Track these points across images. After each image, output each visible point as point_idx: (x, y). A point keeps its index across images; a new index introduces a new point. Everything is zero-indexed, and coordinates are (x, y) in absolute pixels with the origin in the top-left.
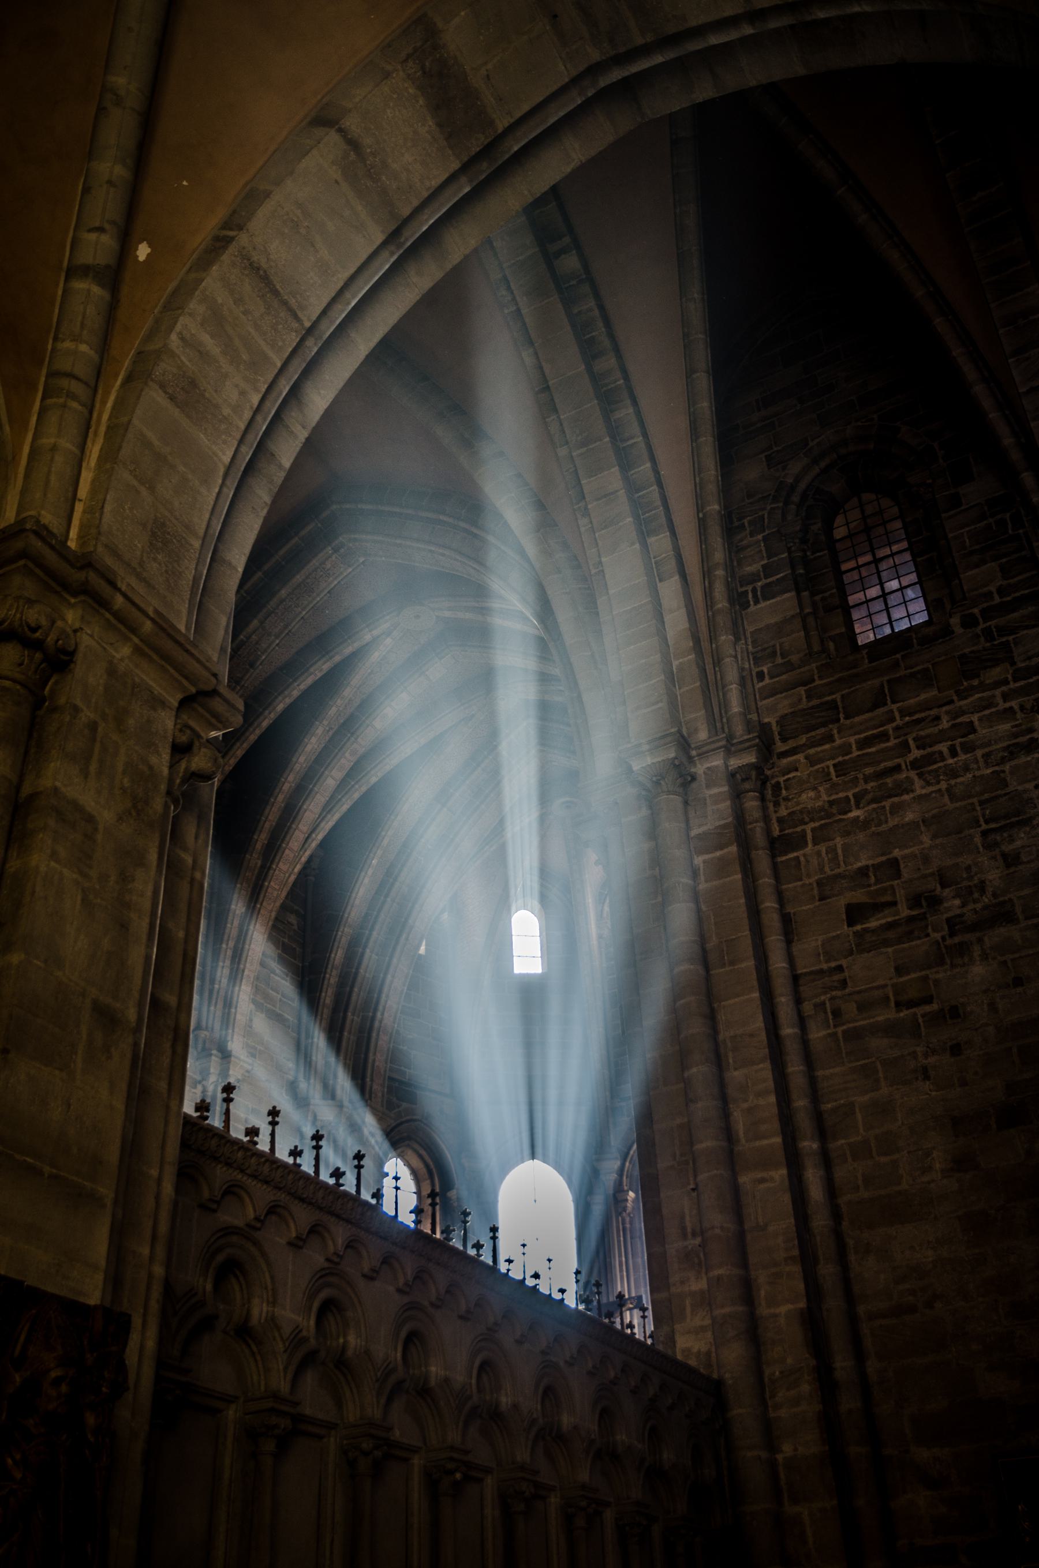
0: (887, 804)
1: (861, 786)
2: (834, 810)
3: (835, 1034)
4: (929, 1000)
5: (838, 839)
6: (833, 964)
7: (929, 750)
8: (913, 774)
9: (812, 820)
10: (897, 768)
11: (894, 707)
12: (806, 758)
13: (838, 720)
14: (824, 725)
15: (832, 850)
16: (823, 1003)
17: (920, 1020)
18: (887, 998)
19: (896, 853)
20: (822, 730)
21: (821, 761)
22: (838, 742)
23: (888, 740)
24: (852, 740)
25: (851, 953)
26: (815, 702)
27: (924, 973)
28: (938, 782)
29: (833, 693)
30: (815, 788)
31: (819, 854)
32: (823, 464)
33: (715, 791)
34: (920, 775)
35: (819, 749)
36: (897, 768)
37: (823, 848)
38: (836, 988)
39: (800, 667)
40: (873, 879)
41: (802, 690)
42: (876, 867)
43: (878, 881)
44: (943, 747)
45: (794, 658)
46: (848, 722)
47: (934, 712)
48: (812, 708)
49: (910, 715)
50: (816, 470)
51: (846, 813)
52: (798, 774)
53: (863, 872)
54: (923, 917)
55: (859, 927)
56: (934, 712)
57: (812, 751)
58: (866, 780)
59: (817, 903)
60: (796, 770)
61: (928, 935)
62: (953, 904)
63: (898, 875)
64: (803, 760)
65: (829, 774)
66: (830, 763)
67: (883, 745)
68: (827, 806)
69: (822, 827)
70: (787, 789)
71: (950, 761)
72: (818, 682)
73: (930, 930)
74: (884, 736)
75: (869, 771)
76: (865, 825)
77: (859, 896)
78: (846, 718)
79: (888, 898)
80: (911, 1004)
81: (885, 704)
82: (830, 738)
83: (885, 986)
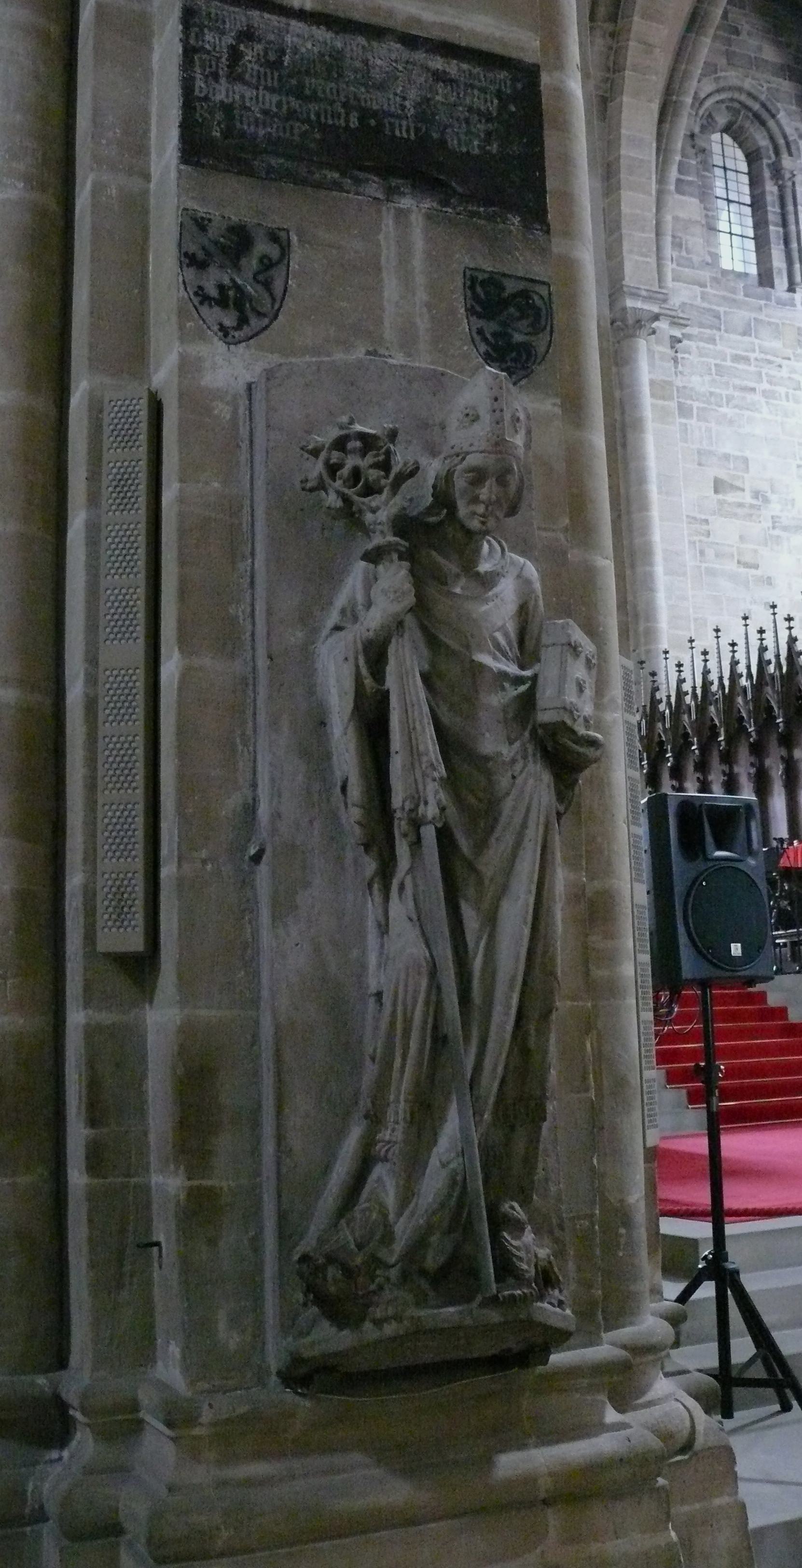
0: (747, 413)
1: (730, 391)
2: (713, 399)
3: (700, 567)
4: (756, 567)
5: (713, 425)
6: (703, 517)
7: (773, 388)
8: (763, 400)
9: (697, 400)
10: (753, 390)
11: (757, 341)
12: (698, 347)
13: (720, 329)
14: (711, 327)
15: (709, 430)
16: (694, 543)
17: (750, 578)
18: (733, 556)
19: (747, 454)
20: (708, 331)
21: (707, 355)
22: (719, 347)
23: (750, 365)
24: (729, 351)
25: (714, 514)
26: (705, 305)
27: (756, 547)
28: (777, 415)
29: (719, 305)
30: (702, 376)
31: (700, 428)
32: (723, 96)
33: (660, 348)
34: (767, 403)
35: (707, 346)
36: (753, 390)
37: (703, 425)
38: (703, 535)
39: (697, 269)
40: (732, 466)
41: (698, 289)
42: (736, 458)
43: (735, 468)
44: (782, 390)
45: (696, 259)
46: (726, 335)
47: (779, 360)
48: (704, 308)
49: (766, 353)
50: (718, 97)
51: (720, 406)
52: (691, 357)
53: (727, 457)
54: (759, 508)
55: (720, 496)
56: (779, 360)
57: (702, 344)
58: (735, 387)
59: (697, 467)
60: (690, 353)
61: (760, 522)
62: (775, 508)
63: (747, 469)
64: (694, 348)
65: (710, 369)
66: (713, 361)
67: (746, 367)
68: (708, 394)
69: (704, 409)
70: (682, 365)
71: (784, 403)
72: (709, 290)
73: (761, 519)
74: (746, 360)
75: (737, 382)
76: (731, 422)
77: (722, 474)
78: (726, 331)
79: (738, 483)
80: (747, 565)
81: (750, 335)
82: (712, 340)
83: (733, 546)
